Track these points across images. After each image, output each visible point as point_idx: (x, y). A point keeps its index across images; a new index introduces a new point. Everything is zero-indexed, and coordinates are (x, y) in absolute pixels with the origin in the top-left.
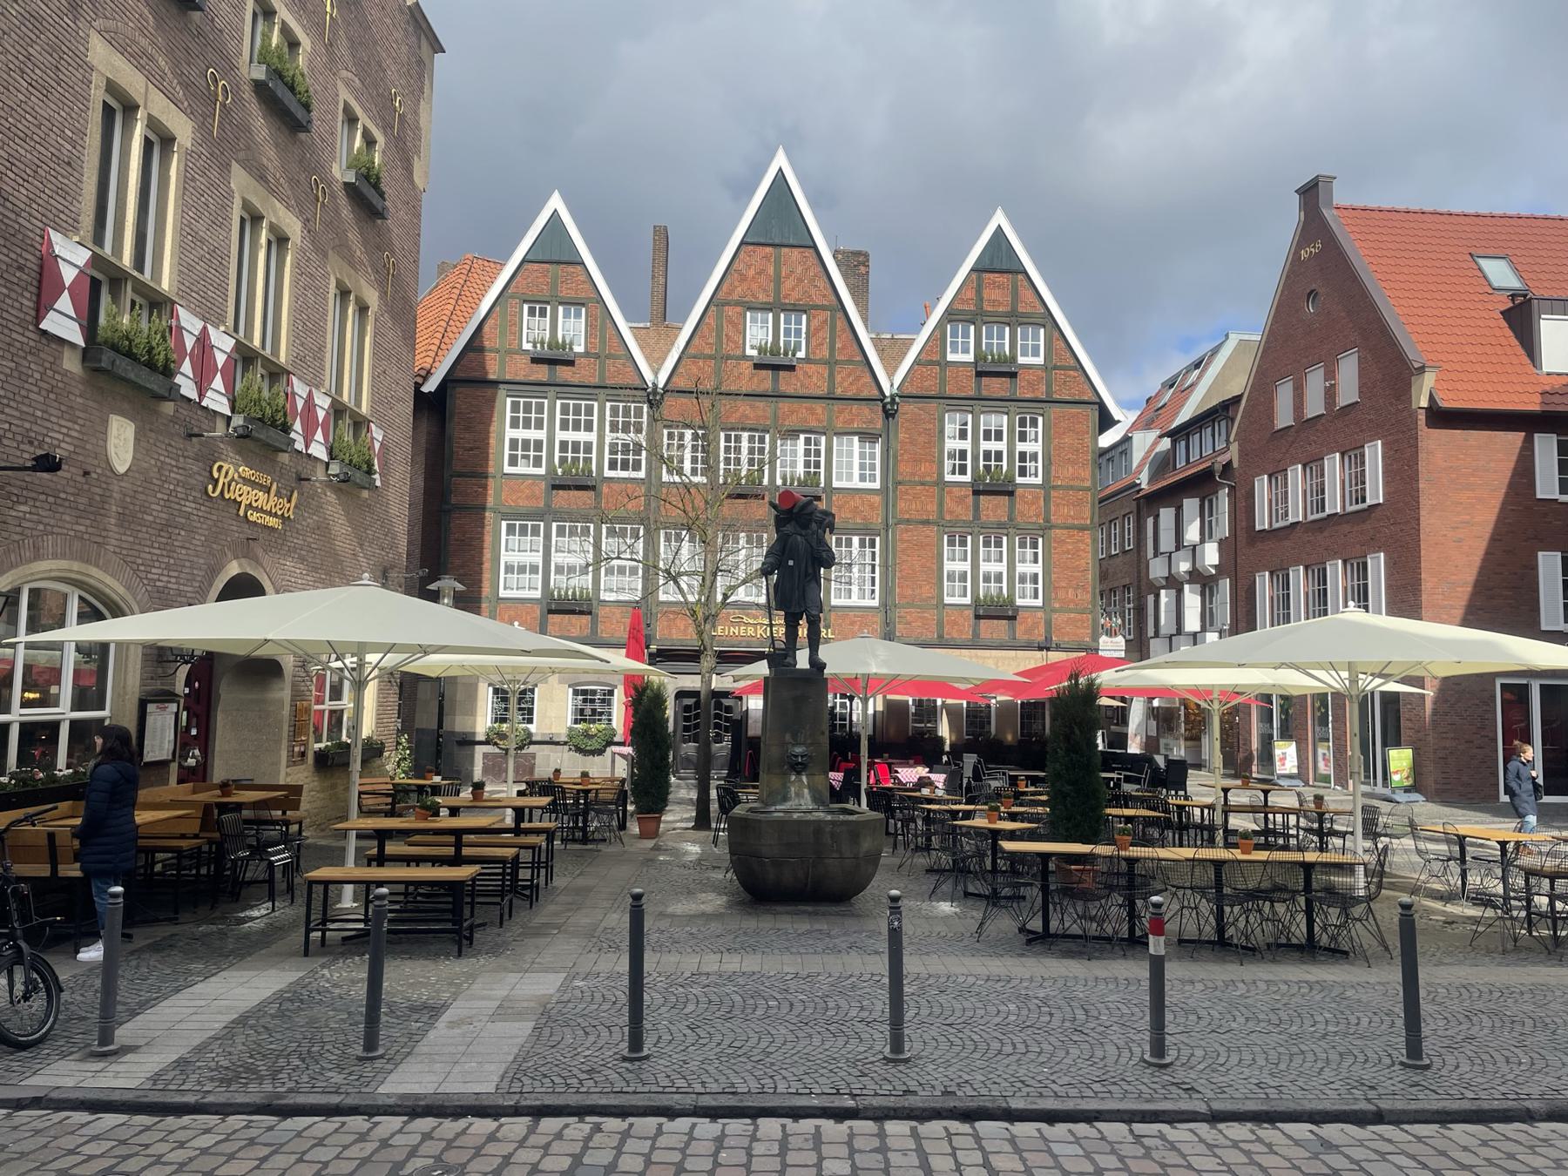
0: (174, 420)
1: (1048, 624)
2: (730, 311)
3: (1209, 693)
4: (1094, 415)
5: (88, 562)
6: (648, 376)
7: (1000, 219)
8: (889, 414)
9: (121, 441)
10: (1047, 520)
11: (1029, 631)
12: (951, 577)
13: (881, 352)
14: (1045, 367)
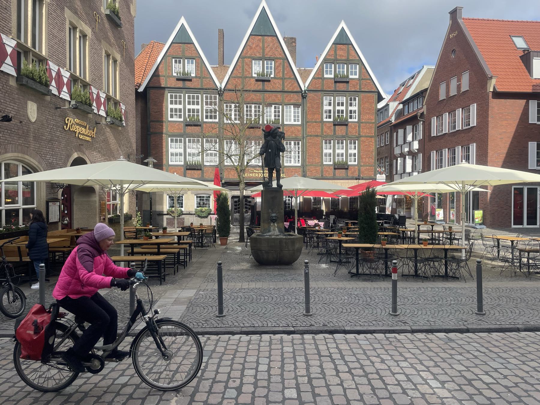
0: (50, 102)
1: (359, 170)
2: (247, 60)
3: (414, 193)
4: (376, 96)
5: (24, 153)
7: (343, 25)
8: (304, 97)
9: (32, 110)
10: (359, 134)
11: (353, 173)
12: (326, 155)
13: (301, 74)
14: (359, 79)
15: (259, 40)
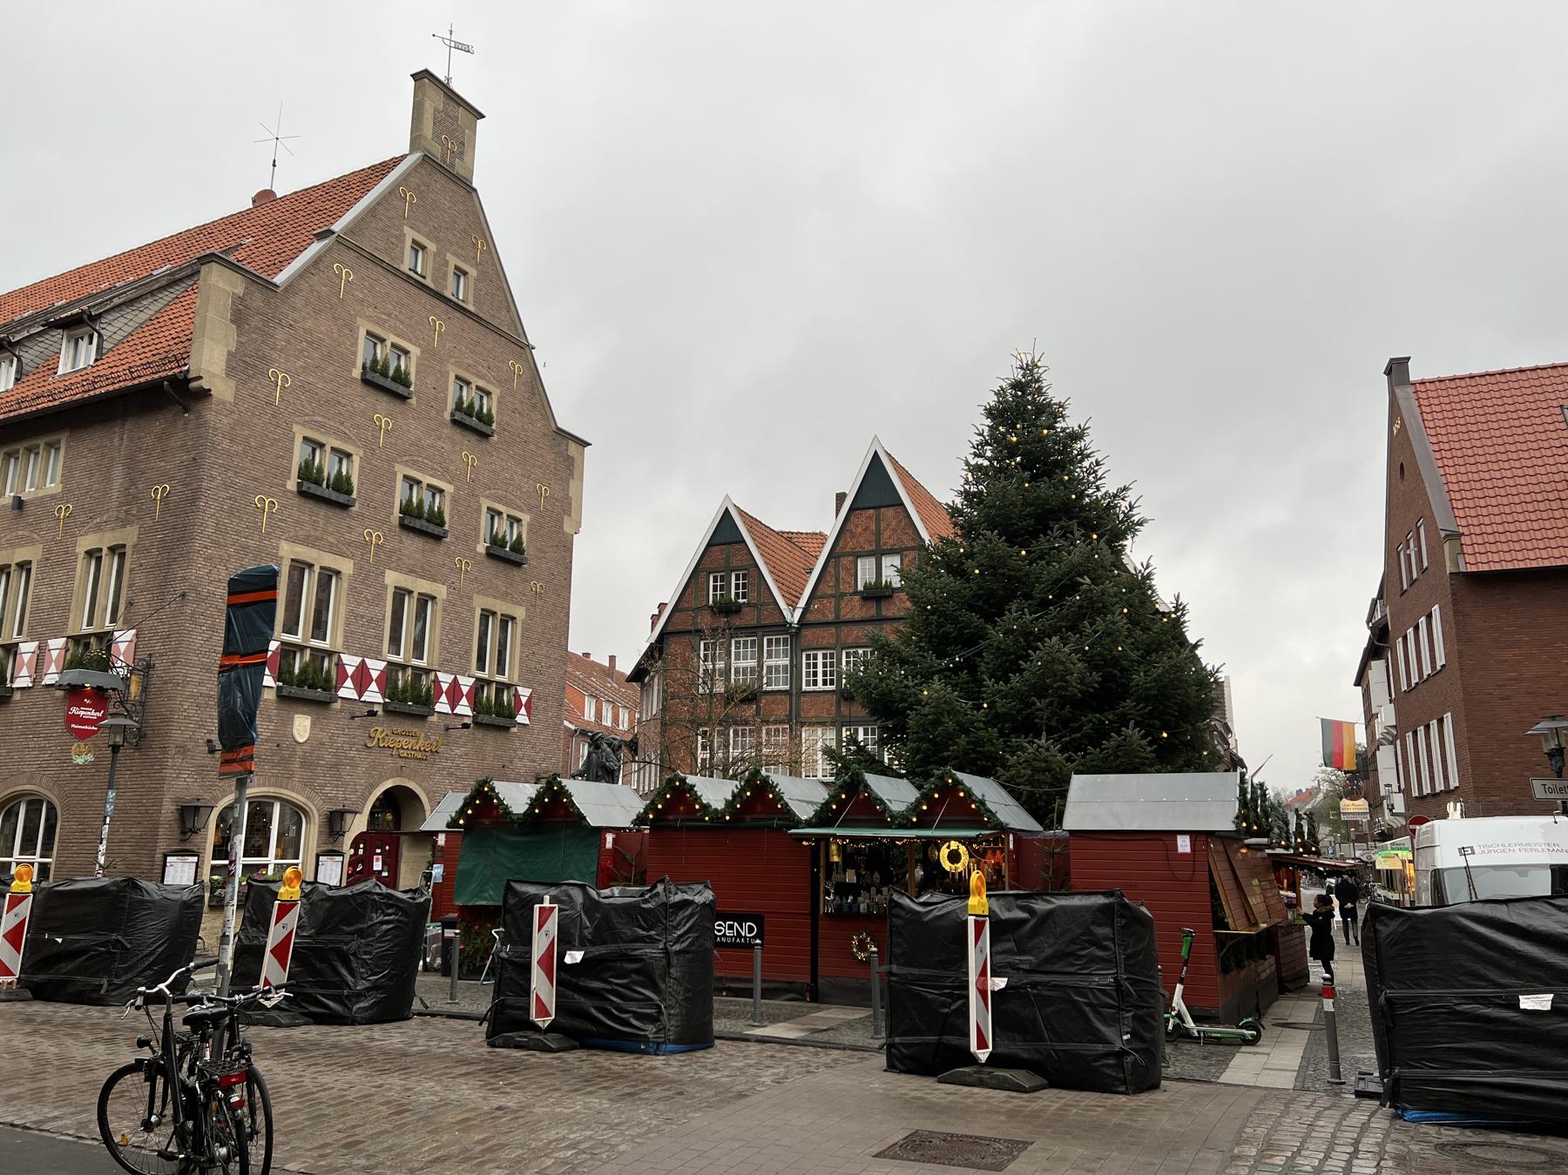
0: (341, 711)
2: (845, 561)
6: (789, 619)
15: (870, 517)
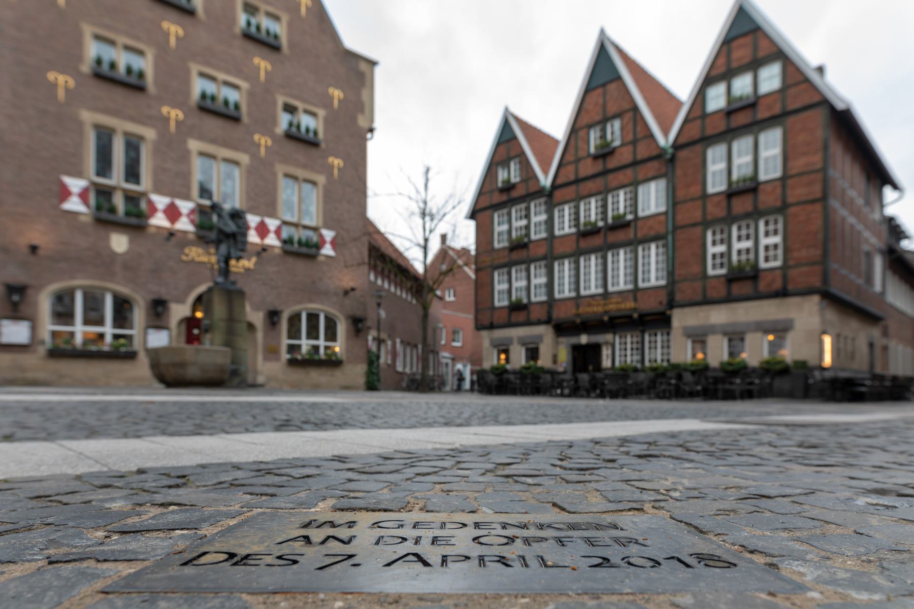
1: (785, 278)
